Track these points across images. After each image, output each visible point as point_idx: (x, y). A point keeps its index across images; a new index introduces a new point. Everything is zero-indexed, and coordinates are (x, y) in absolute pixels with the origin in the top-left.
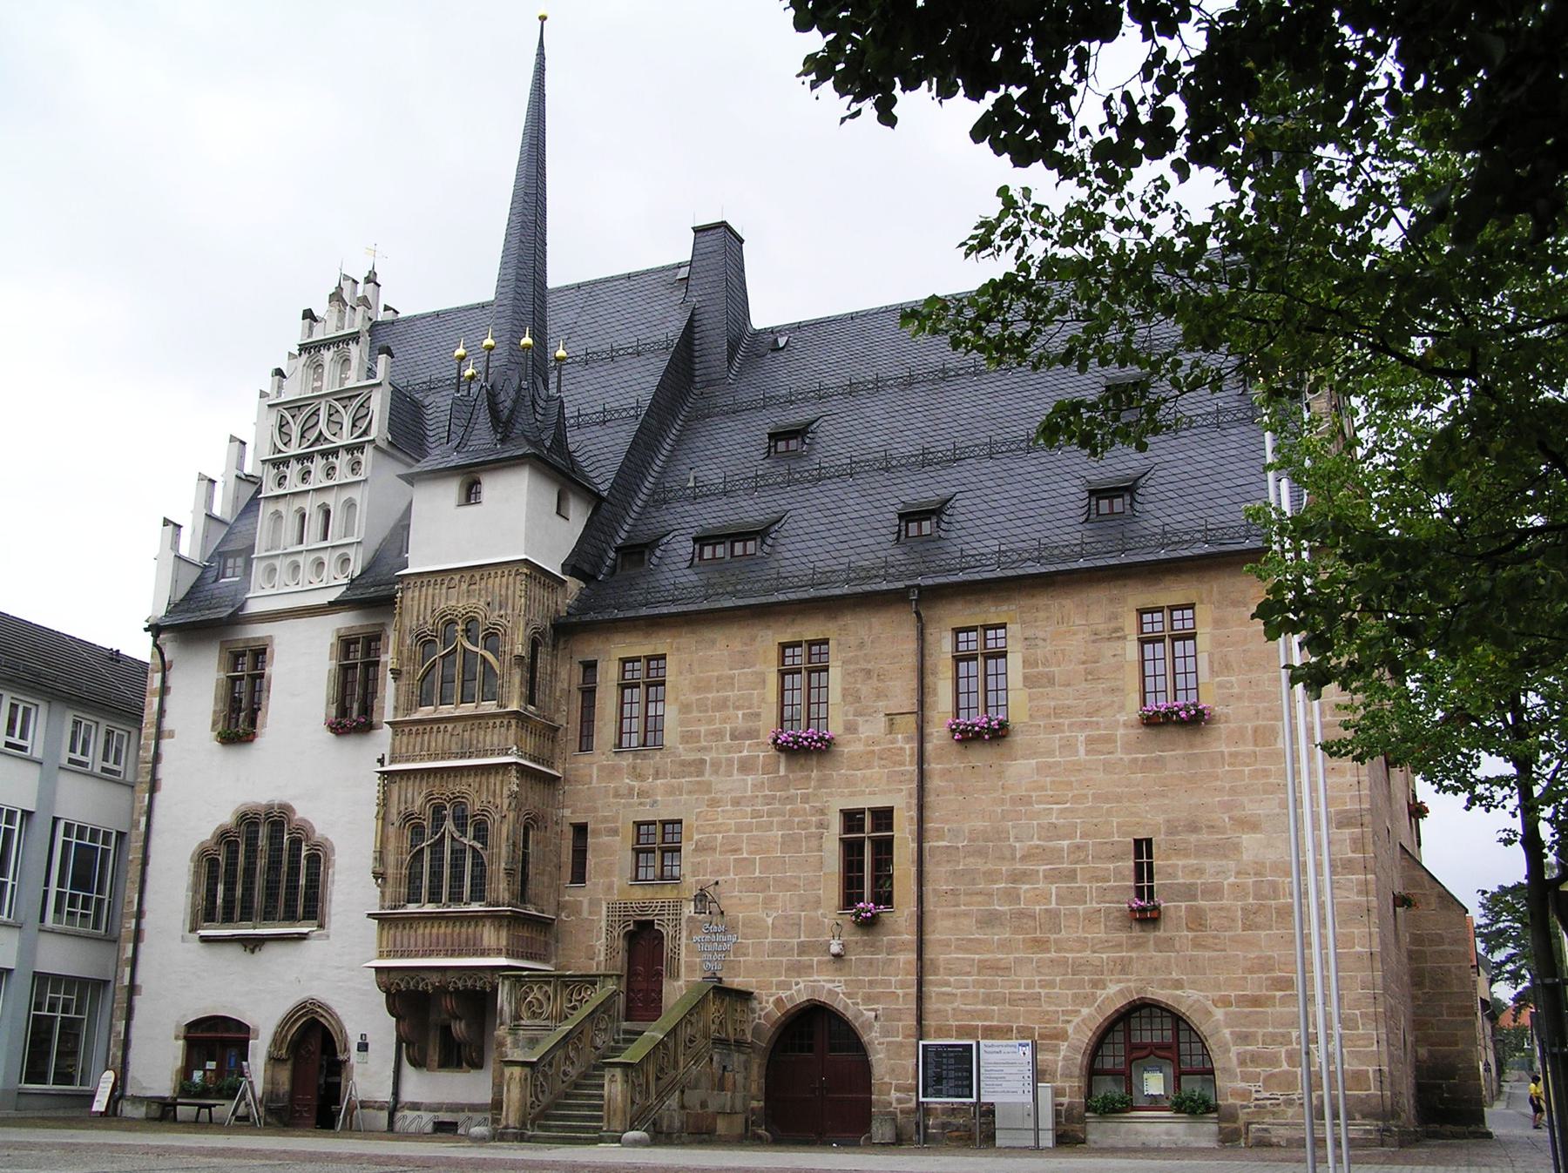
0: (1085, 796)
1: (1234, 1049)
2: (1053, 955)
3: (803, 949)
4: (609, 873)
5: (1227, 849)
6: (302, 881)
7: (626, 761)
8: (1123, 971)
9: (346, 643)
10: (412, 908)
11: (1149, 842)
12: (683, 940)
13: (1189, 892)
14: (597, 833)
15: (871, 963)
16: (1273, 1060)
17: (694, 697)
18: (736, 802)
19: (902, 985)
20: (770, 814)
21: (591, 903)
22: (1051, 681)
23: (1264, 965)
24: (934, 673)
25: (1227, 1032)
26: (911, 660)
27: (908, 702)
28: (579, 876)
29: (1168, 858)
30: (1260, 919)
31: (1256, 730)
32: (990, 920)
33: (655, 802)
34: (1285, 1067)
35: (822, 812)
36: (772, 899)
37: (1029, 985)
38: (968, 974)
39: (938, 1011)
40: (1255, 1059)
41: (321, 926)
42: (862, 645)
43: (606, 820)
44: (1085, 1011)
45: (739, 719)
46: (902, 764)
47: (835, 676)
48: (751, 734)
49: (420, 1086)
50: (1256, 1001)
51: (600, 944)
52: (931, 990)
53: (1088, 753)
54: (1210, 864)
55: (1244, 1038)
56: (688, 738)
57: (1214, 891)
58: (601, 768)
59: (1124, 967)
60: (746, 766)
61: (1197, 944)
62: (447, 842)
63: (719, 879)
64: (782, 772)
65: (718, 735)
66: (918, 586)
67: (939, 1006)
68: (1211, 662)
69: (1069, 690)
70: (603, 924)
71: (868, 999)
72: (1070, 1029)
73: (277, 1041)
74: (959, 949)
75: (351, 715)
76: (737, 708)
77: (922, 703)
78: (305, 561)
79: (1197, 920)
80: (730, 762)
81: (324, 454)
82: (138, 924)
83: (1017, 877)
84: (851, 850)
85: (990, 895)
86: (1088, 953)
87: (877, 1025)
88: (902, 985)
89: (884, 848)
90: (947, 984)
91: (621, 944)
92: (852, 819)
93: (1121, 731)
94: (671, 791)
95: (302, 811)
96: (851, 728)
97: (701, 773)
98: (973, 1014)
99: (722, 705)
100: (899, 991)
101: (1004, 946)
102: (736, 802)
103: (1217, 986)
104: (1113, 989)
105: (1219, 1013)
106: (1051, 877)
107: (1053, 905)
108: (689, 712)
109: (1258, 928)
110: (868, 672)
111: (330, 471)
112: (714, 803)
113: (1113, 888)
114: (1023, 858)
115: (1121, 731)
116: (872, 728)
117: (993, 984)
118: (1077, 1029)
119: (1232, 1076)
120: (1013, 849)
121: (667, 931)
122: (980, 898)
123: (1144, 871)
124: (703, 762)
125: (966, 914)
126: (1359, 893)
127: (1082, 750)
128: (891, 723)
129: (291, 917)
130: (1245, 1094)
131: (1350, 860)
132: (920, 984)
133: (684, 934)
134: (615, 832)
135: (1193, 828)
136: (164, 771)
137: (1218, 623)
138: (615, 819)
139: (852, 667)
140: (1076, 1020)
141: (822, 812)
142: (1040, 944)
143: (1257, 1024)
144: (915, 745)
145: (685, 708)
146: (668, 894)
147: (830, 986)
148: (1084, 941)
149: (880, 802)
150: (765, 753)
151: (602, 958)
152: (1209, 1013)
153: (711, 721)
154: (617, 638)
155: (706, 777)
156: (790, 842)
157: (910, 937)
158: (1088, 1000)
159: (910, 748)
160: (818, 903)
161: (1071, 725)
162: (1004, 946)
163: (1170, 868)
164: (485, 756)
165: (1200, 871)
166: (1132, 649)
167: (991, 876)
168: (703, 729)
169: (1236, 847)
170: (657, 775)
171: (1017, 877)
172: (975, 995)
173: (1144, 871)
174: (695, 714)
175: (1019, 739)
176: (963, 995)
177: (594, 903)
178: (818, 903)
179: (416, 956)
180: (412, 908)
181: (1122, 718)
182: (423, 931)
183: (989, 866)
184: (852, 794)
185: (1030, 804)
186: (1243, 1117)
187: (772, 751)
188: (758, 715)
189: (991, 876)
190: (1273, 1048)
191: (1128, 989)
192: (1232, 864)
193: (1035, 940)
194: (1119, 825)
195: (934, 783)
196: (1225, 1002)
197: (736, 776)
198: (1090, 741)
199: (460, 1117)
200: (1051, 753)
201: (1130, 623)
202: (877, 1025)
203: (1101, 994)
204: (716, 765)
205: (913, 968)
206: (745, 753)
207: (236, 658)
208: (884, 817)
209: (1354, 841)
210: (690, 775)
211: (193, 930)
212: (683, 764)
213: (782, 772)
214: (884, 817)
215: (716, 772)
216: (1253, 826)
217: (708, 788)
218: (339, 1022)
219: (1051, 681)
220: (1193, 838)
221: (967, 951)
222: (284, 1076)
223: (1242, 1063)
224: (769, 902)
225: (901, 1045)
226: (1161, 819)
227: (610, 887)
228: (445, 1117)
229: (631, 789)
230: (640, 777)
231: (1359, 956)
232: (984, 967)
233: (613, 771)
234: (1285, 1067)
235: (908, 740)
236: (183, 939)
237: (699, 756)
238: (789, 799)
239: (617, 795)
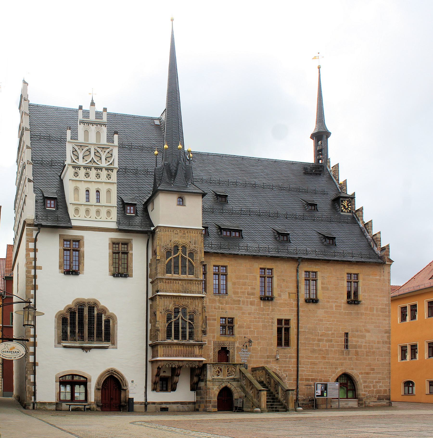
0: (335, 320)
1: (363, 384)
2: (327, 361)
3: (268, 357)
4: (213, 332)
5: (363, 337)
6: (103, 328)
7: (217, 298)
8: (342, 365)
9: (114, 243)
10: (169, 341)
11: (347, 333)
12: (236, 353)
13: (355, 347)
14: (209, 319)
15: (285, 361)
16: (370, 387)
17: (236, 281)
18: (249, 314)
19: (293, 367)
20: (259, 318)
21: (208, 341)
22: (328, 289)
23: (369, 365)
24: (300, 283)
25: (361, 381)
26: (294, 278)
27: (294, 290)
28: (204, 332)
29: (351, 338)
30: (369, 354)
31: (370, 308)
32: (313, 351)
33: (226, 311)
34: (372, 389)
35: (272, 319)
36: (260, 343)
37: (322, 368)
38: (308, 365)
39: (301, 374)
40: (367, 387)
41: (113, 344)
42: (282, 272)
43: (212, 316)
44: (334, 375)
45: (249, 289)
46: (293, 307)
47: (275, 279)
48: (253, 294)
49: (156, 397)
50: (368, 373)
51: (211, 354)
52: (300, 369)
53: (336, 309)
54: (360, 340)
55: (365, 382)
56: (235, 293)
57: (360, 347)
58: (210, 299)
59: (342, 364)
60: (252, 303)
61: (357, 360)
62: (180, 320)
63: (245, 336)
64: (262, 306)
65: (243, 293)
66: (302, 258)
67: (301, 373)
68: (362, 289)
69: (332, 292)
70: (212, 348)
71: (284, 371)
72: (330, 379)
73: (98, 383)
74: (306, 358)
75: (120, 270)
76: (249, 286)
77: (298, 292)
78: (93, 210)
79: (357, 353)
80: (247, 301)
81: (96, 168)
82: (35, 340)
83: (319, 340)
84: (279, 330)
85: (313, 344)
86: (334, 361)
87: (287, 378)
88: (293, 367)
89: (287, 330)
90: (303, 367)
91: (217, 354)
92: (280, 321)
93: (343, 305)
94: (231, 309)
95: (103, 303)
96: (280, 295)
97: (239, 304)
98: (309, 375)
99: (244, 284)
100: (292, 369)
101: (316, 358)
102: (249, 314)
103: (360, 370)
104: (339, 370)
105: (360, 376)
106: (328, 341)
107: (327, 348)
108: (235, 285)
109: (369, 356)
110: (284, 280)
111: (98, 176)
112: (243, 313)
113: (340, 345)
114: (321, 335)
115: (343, 305)
116: (285, 296)
117: (314, 368)
118: (332, 379)
119: (362, 391)
120: (318, 332)
121: (231, 351)
122: (311, 345)
123: (347, 341)
124: (239, 301)
125: (308, 349)
126: (388, 349)
127: (334, 308)
128: (289, 296)
129: (99, 339)
130: (364, 395)
131: (387, 341)
132: (298, 367)
133: (236, 352)
134: (215, 320)
135: (357, 331)
136: (39, 282)
137: (364, 280)
138: (215, 316)
139: (280, 278)
140: (332, 377)
141: (272, 319)
142: (324, 358)
143: (367, 379)
144: (296, 302)
145: (234, 284)
146: (231, 339)
147: (275, 367)
148: (333, 358)
149: (287, 318)
150: (257, 300)
151: (212, 358)
152: (358, 376)
153: (242, 288)
154: (213, 258)
155: (241, 305)
156: (264, 327)
157: (295, 355)
158: (334, 372)
159: (295, 303)
160: (272, 344)
161: (332, 301)
162: (316, 358)
163: (352, 340)
164: (193, 293)
165: (358, 342)
166: (345, 284)
167: (314, 340)
168: (239, 291)
169: (365, 336)
170: (226, 304)
171: (319, 340)
172: (310, 370)
173: (347, 341)
174: (237, 286)
175: (320, 303)
176: (307, 370)
177: (209, 341)
178: (272, 344)
179: (173, 356)
180: (169, 341)
181: (343, 301)
182: (175, 348)
183: (313, 337)
184: (280, 314)
185: (322, 321)
186: (364, 400)
187: (259, 300)
188: (255, 288)
189: (314, 340)
190: (370, 384)
191: (342, 370)
192: (364, 340)
193: (323, 357)
194: (342, 329)
195: (300, 313)
196: (361, 373)
197: (249, 306)
198: (336, 306)
199: (168, 406)
200: (327, 308)
201: (345, 277)
202: (287, 378)
203: (337, 371)
204: (243, 302)
205: (296, 363)
206: (251, 299)
207: (65, 240)
208: (287, 321)
209: (388, 337)
210: (236, 304)
211: (59, 343)
212: (234, 301)
213: (262, 306)
214: (287, 321)
215: (243, 304)
216: (368, 331)
217: (240, 309)
218: (122, 376)
219: (328, 289)
220: (357, 333)
221: (308, 359)
222: (99, 394)
223: (364, 388)
224: (259, 343)
225: (292, 383)
226: (350, 328)
227: (214, 337)
228: (164, 406)
229: (219, 307)
230: (222, 303)
231: (387, 363)
232: (312, 363)
233: (213, 301)
234: (372, 389)
235: (294, 301)
236: (55, 347)
237: (239, 299)
238: (264, 314)
239: (215, 308)
